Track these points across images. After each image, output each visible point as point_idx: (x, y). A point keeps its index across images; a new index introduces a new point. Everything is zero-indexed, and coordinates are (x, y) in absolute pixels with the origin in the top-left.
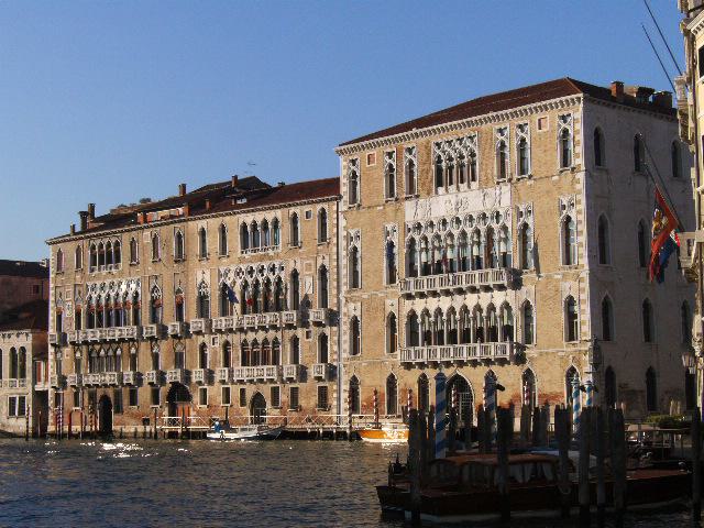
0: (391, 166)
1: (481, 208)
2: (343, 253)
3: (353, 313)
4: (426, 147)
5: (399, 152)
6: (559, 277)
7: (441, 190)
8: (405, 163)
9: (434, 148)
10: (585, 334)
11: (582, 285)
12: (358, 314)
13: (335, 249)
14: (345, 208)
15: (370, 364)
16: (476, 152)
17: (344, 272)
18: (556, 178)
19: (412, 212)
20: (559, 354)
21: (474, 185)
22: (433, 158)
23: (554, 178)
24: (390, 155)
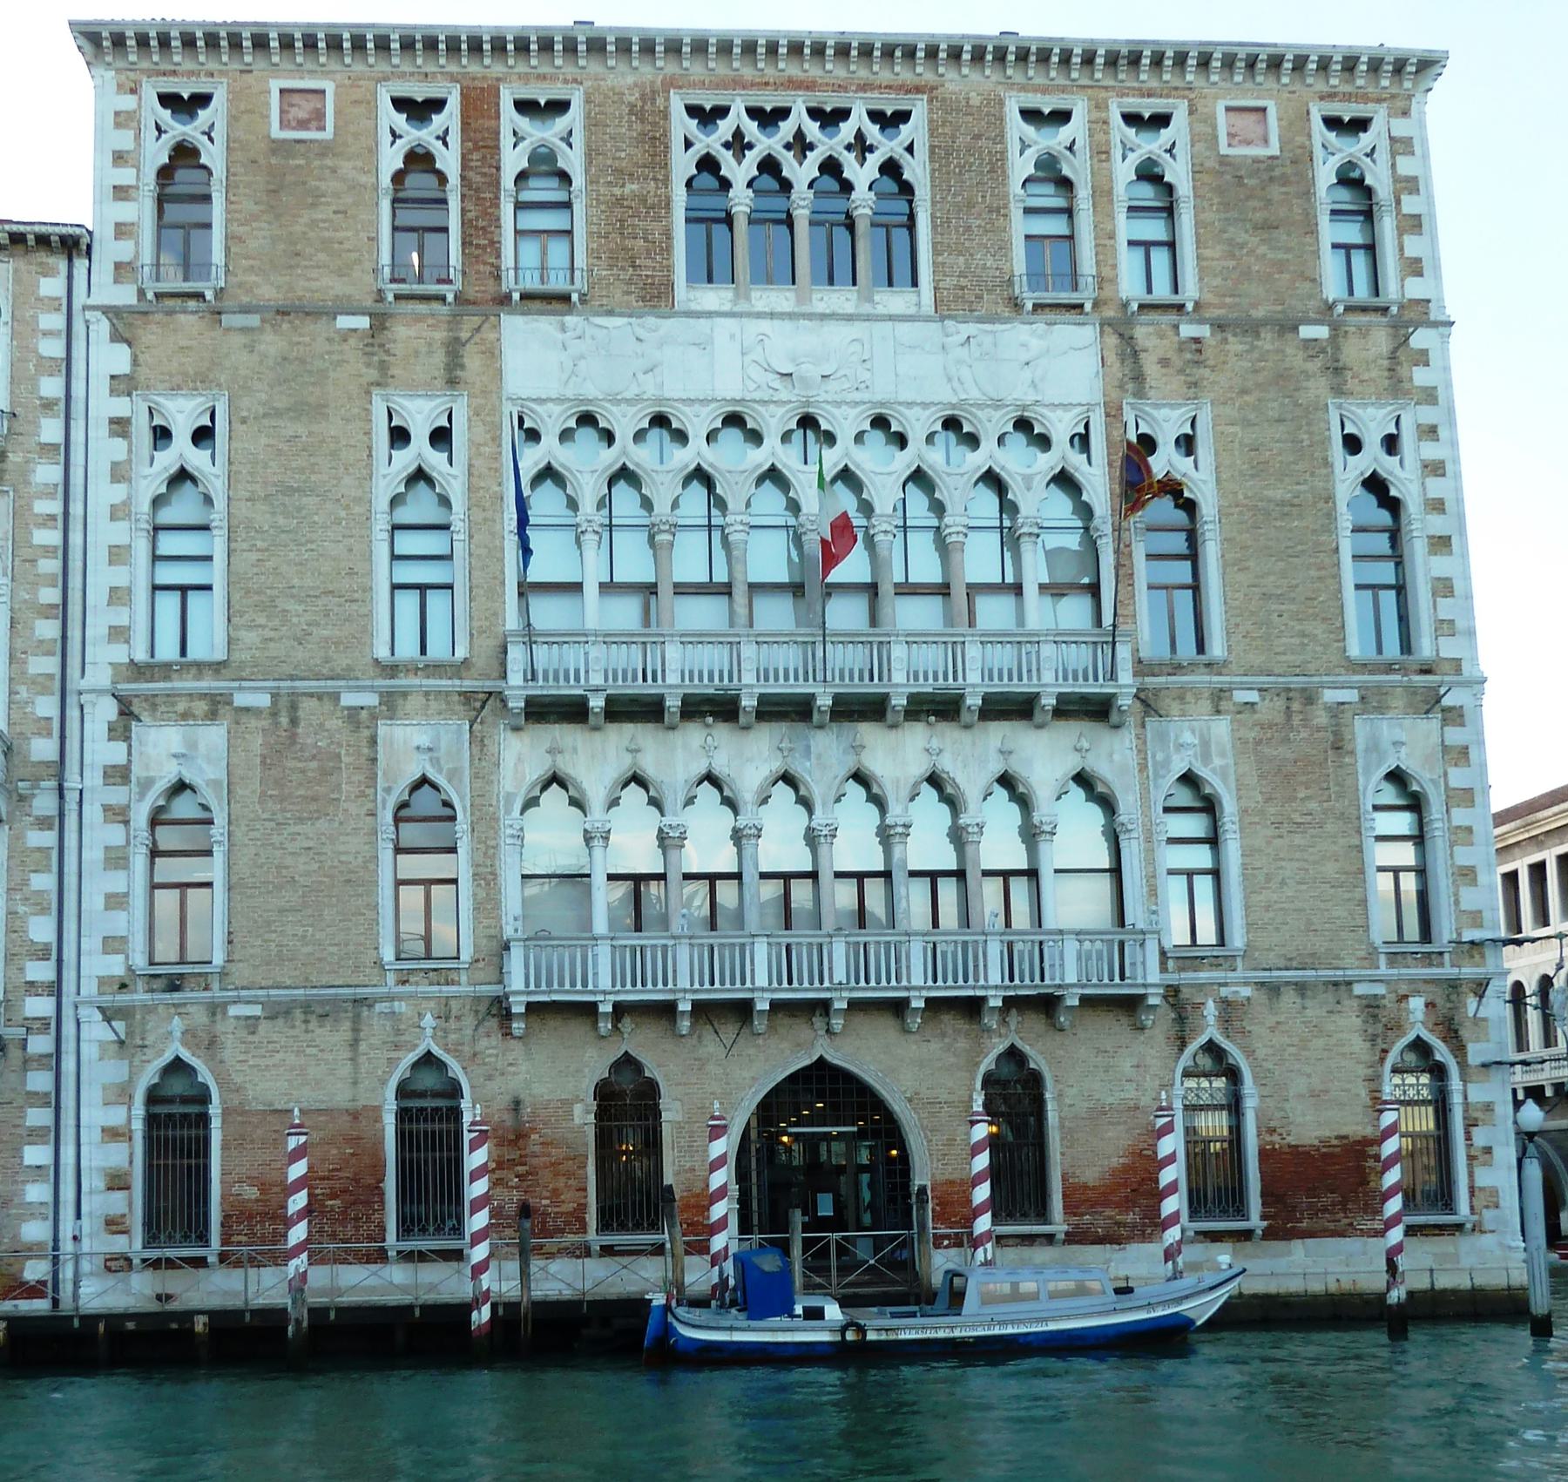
0: (419, 160)
1: (946, 396)
2: (105, 494)
3: (168, 773)
4: (636, 112)
5: (479, 105)
6: (1351, 696)
7: (713, 297)
8: (513, 160)
9: (682, 124)
10: (1476, 919)
11: (1454, 736)
12: (207, 773)
13: (47, 473)
14: (125, 296)
15: (278, 1012)
16: (916, 171)
17: (103, 577)
18: (1322, 332)
19: (536, 361)
20: (1358, 989)
21: (896, 301)
22: (683, 165)
23: (1306, 332)
24: (419, 110)
